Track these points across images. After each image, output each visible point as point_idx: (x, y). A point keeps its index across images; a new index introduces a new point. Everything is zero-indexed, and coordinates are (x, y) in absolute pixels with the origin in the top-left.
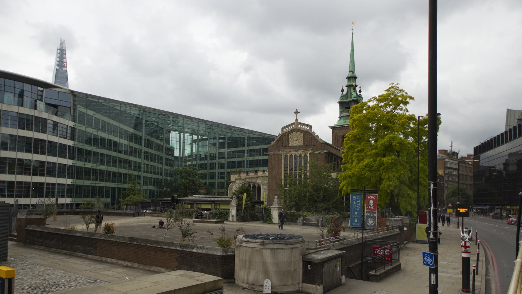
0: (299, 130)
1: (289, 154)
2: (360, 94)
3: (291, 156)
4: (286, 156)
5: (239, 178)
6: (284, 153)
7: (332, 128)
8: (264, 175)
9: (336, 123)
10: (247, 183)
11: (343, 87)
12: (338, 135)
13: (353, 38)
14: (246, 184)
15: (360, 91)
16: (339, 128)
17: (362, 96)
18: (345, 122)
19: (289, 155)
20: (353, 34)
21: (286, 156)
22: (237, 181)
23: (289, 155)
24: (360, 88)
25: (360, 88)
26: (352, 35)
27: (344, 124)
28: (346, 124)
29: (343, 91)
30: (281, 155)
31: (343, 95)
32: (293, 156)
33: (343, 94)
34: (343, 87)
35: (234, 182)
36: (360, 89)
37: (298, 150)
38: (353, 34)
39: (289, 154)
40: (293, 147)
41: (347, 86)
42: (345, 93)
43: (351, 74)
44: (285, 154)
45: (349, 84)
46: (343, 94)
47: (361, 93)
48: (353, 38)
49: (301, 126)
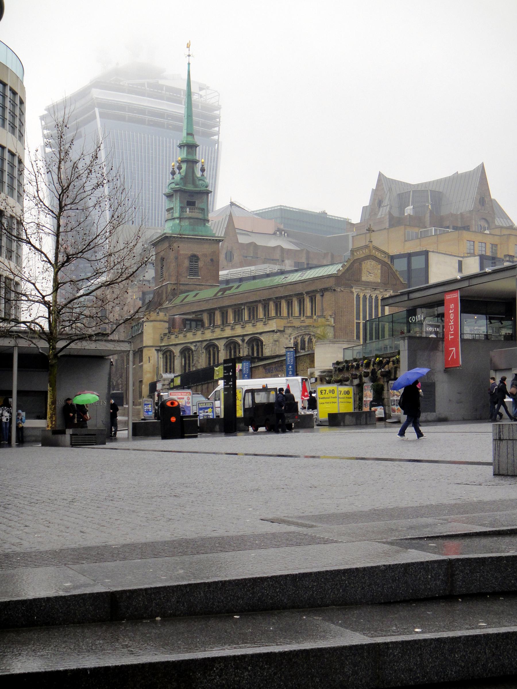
0: (375, 259)
1: (362, 293)
3: (365, 296)
4: (358, 296)
5: (289, 325)
6: (358, 290)
8: (328, 323)
10: (301, 335)
12: (181, 252)
14: (298, 336)
16: (183, 239)
18: (193, 230)
19: (361, 296)
20: (189, 64)
21: (358, 296)
22: (286, 331)
23: (361, 296)
26: (187, 65)
27: (192, 233)
28: (196, 233)
30: (352, 292)
32: (368, 297)
35: (284, 331)
37: (375, 289)
38: (189, 64)
39: (362, 293)
40: (367, 284)
43: (190, 140)
44: (357, 294)
49: (377, 253)
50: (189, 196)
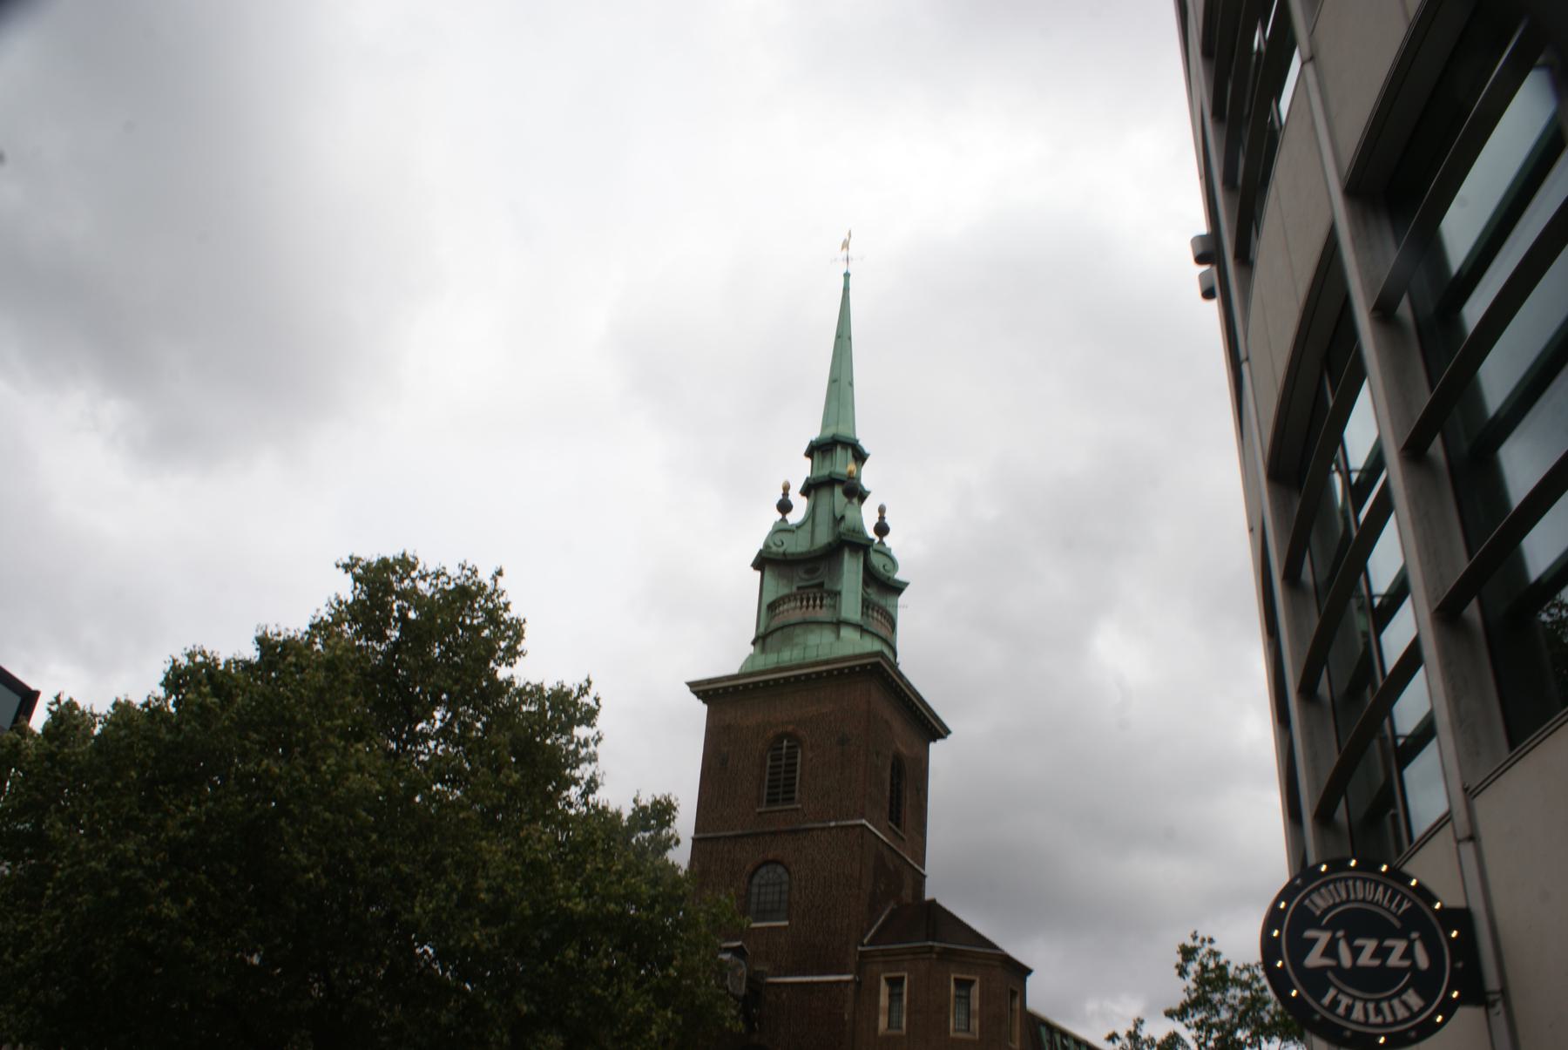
2: (881, 542)
7: (705, 690)
9: (734, 669)
11: (786, 489)
13: (846, 290)
15: (882, 529)
17: (894, 553)
20: (847, 275)
24: (882, 510)
25: (882, 510)
26: (842, 280)
29: (785, 507)
31: (783, 526)
33: (784, 520)
34: (786, 489)
36: (882, 518)
38: (847, 275)
41: (809, 489)
42: (796, 516)
45: (825, 471)
46: (784, 520)
47: (886, 539)
48: (846, 290)
50: (807, 572)
